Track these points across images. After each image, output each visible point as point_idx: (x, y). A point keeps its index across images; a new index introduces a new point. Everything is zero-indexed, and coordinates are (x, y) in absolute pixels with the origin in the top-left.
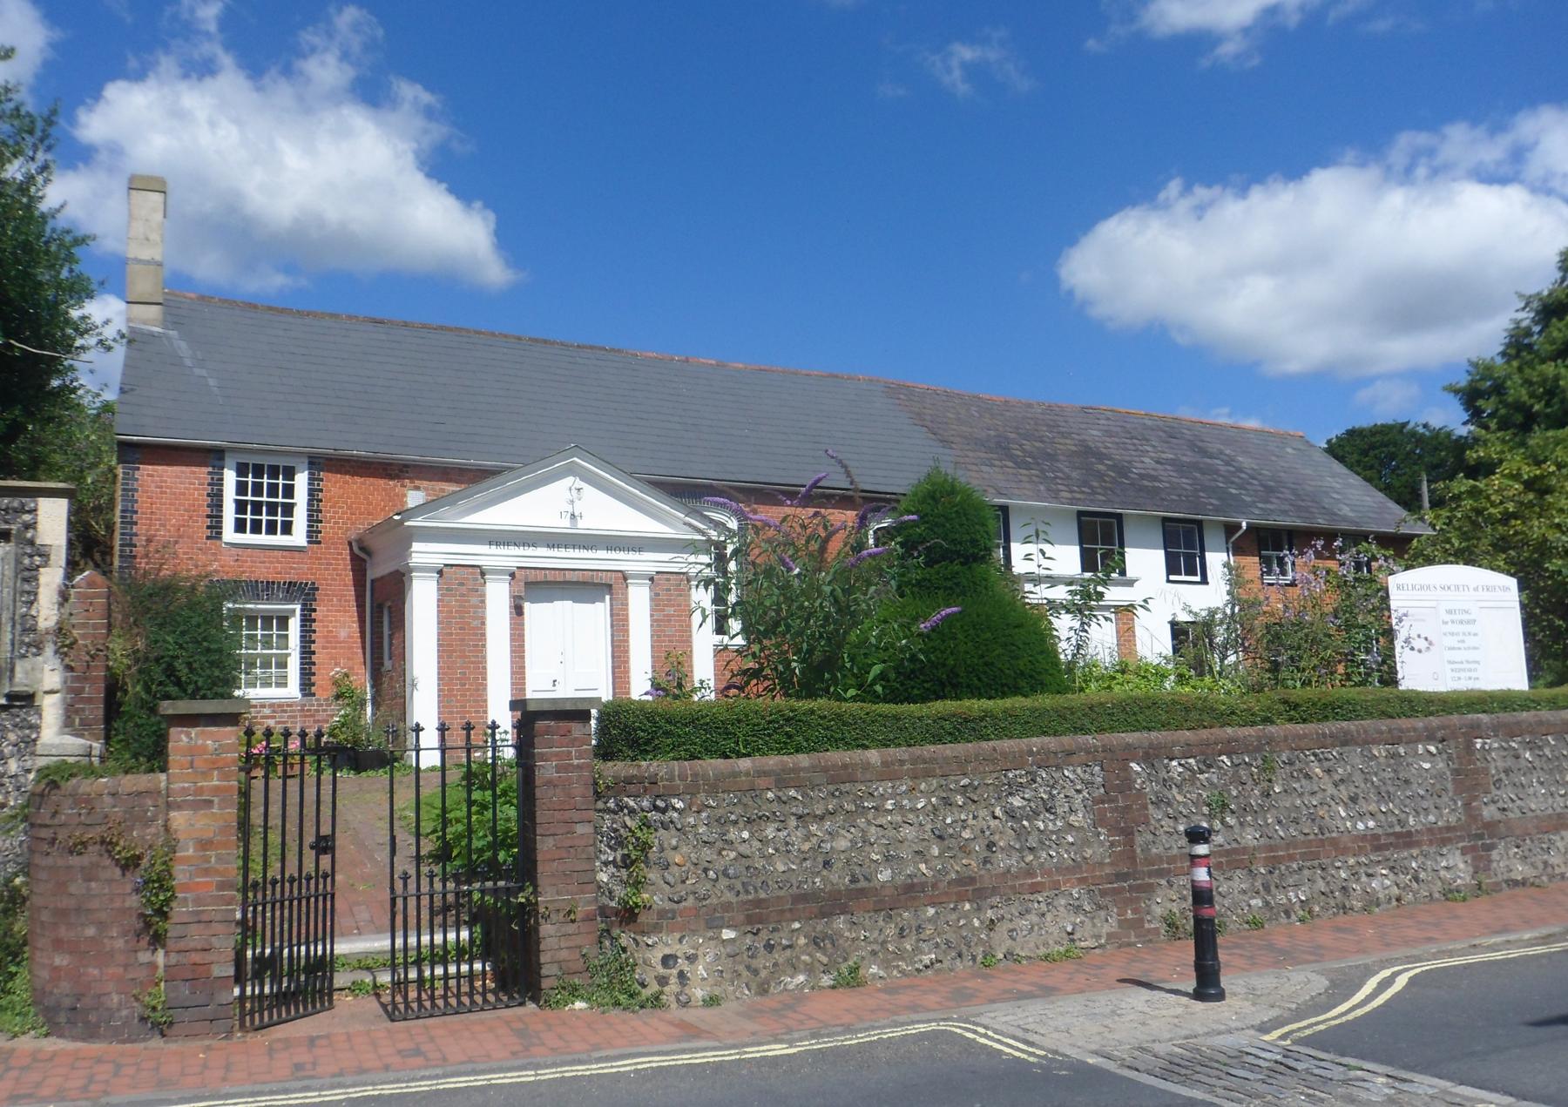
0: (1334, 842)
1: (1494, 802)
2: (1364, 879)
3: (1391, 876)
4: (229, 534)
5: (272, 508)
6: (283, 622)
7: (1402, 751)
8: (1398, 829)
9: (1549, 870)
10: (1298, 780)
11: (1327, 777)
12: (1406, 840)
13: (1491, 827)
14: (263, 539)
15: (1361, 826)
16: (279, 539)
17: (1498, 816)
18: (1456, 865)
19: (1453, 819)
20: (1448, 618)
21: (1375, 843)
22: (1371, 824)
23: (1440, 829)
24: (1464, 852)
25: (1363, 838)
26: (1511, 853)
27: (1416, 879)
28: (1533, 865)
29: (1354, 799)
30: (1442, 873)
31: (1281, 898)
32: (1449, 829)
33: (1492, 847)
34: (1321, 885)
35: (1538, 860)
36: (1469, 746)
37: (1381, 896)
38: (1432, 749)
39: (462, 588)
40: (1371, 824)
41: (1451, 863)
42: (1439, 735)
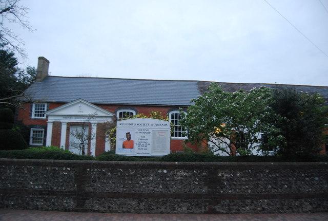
0: (26, 190)
1: (90, 186)
2: (35, 201)
3: (45, 202)
4: (33, 117)
5: (41, 112)
6: (42, 132)
7: (57, 169)
8: (50, 190)
9: (111, 209)
10: (19, 173)
11: (29, 173)
12: (52, 193)
13: (88, 195)
14: (39, 117)
15: (37, 187)
16: (42, 118)
17: (92, 190)
18: (72, 203)
19: (72, 189)
20: (139, 131)
21: (41, 192)
22: (40, 187)
23: (66, 192)
24: (74, 199)
25: (36, 190)
26: (94, 202)
27: (53, 204)
28: (104, 207)
29: (36, 180)
30: (64, 204)
31: (6, 202)
32: (69, 192)
33: (86, 199)
34: (20, 201)
35: (107, 205)
36: (85, 170)
37: (39, 207)
38: (69, 169)
39: (57, 126)
40: (40, 187)
41: (68, 201)
42: (73, 166)
